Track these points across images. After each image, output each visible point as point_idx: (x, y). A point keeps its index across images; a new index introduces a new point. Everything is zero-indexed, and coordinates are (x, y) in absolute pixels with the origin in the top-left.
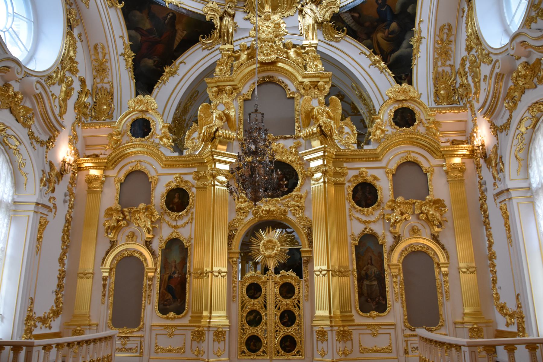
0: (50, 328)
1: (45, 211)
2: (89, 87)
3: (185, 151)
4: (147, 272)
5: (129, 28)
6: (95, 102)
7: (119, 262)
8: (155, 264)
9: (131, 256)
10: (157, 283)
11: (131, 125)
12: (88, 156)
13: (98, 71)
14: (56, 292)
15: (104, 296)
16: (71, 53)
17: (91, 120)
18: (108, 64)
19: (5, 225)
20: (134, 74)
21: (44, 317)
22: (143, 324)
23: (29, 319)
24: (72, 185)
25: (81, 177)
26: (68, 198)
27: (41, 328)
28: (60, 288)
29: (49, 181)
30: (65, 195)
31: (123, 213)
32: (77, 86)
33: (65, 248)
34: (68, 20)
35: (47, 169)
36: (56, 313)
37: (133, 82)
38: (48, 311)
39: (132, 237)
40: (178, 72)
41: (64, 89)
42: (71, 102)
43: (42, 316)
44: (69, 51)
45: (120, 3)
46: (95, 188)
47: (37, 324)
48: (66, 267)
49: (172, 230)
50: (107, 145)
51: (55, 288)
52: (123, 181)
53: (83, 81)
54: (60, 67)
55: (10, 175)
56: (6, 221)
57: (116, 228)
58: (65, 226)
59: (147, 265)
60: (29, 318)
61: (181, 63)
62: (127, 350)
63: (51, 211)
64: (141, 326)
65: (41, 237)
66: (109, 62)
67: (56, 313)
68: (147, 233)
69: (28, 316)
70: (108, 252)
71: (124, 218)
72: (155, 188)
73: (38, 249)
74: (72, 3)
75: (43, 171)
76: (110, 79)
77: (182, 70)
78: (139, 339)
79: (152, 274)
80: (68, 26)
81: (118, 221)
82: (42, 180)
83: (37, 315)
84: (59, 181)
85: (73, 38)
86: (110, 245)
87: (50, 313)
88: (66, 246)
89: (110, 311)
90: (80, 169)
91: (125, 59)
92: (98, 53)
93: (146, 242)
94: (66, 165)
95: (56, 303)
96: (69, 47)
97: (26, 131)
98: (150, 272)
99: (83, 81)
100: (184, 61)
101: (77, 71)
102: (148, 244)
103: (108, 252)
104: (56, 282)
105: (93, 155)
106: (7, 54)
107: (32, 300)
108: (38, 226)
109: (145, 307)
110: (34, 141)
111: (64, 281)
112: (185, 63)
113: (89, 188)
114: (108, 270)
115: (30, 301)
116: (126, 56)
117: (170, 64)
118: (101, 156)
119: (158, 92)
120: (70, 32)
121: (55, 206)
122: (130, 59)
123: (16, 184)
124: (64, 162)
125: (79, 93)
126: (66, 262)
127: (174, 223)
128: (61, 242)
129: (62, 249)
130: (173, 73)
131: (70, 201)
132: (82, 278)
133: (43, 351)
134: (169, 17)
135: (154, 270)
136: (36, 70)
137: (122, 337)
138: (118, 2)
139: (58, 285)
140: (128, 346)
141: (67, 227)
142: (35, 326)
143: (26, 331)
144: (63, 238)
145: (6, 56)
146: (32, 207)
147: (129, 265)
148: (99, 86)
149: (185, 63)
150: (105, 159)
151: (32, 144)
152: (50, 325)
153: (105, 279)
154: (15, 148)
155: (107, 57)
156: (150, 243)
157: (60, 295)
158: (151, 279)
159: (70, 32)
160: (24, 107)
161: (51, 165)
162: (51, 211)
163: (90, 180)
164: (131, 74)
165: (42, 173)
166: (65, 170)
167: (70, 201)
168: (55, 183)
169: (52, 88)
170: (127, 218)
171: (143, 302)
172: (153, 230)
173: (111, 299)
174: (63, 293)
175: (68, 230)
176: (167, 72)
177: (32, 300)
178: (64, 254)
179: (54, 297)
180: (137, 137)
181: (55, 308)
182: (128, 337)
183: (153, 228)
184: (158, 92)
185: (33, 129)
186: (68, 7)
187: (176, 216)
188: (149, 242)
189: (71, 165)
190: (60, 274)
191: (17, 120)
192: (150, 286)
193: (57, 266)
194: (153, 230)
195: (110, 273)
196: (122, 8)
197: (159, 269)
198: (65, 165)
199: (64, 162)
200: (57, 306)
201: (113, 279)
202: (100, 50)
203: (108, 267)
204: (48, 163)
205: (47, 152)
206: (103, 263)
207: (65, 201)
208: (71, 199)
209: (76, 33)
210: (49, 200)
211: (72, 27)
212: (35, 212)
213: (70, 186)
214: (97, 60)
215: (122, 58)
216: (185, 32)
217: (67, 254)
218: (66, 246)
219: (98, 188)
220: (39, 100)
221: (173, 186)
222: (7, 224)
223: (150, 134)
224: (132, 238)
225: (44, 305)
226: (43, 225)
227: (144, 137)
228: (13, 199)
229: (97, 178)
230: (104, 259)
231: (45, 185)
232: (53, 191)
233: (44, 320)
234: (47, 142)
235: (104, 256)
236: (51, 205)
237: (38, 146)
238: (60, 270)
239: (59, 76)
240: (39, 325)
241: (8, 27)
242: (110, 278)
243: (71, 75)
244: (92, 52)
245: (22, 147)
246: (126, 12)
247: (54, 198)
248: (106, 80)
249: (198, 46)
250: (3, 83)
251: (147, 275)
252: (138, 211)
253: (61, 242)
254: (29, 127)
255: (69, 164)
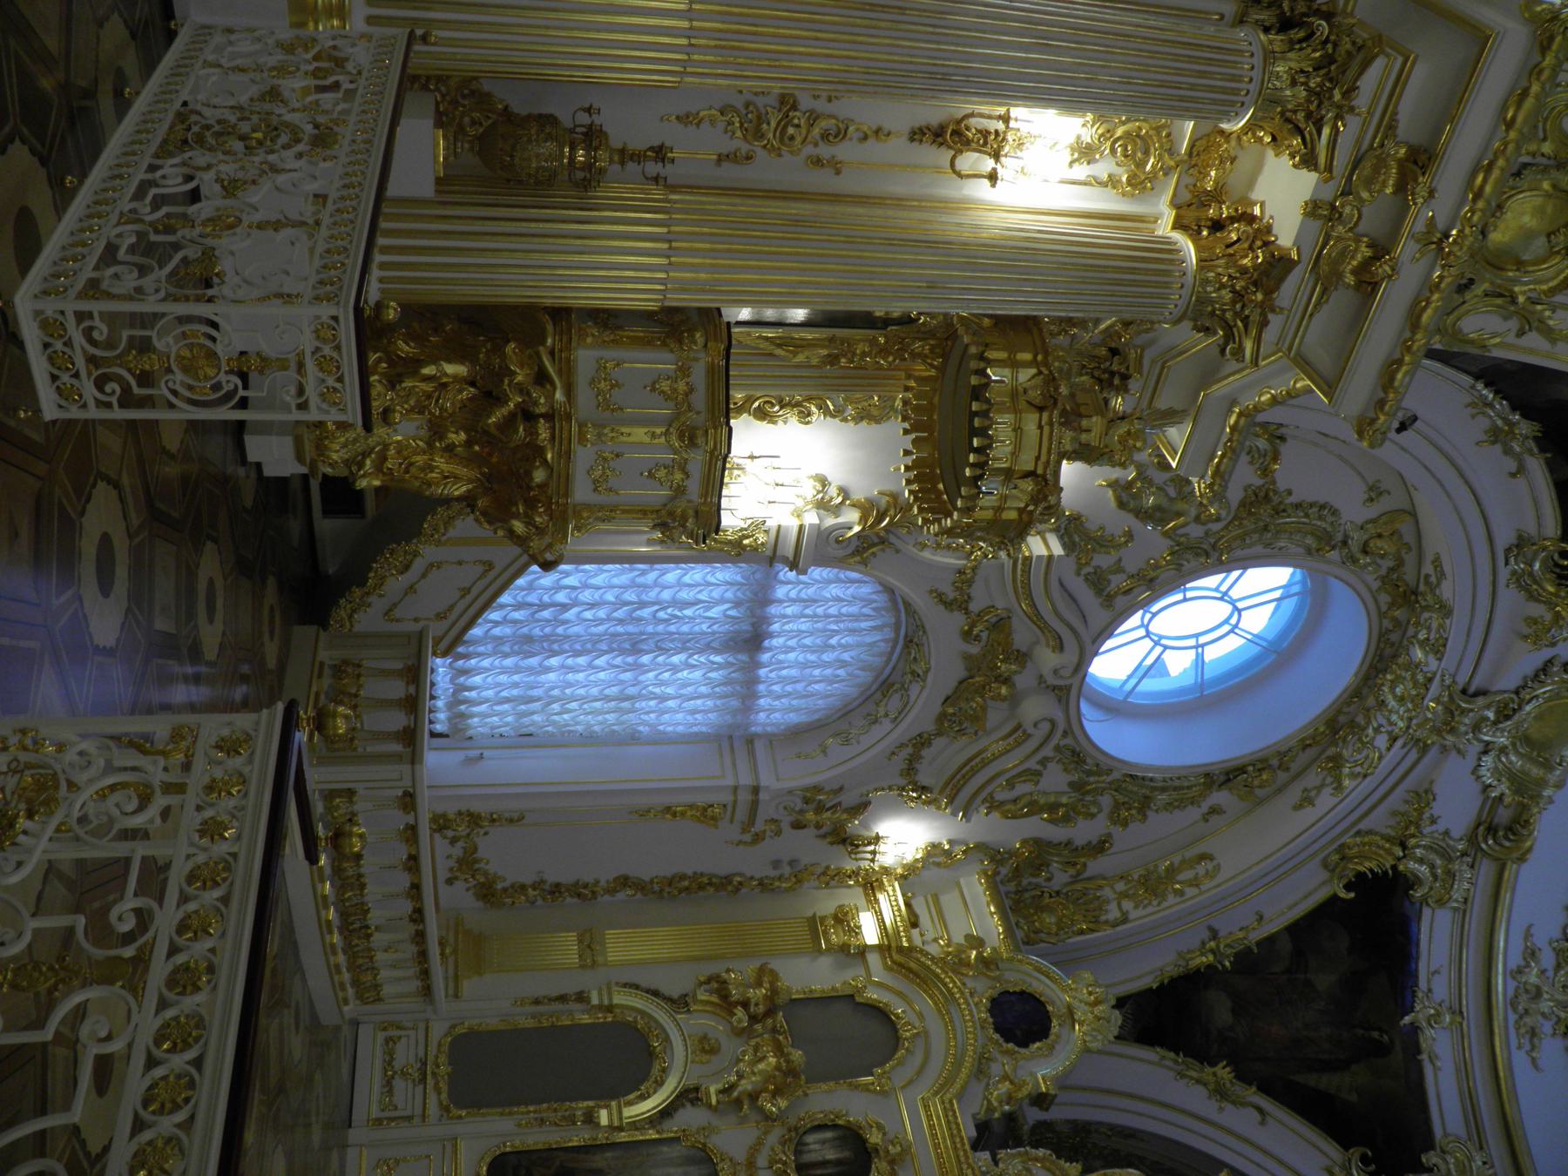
0: (450, 882)
1: (742, 813)
2: (1095, 866)
3: (986, 1155)
4: (607, 1107)
5: (1294, 929)
6: (1058, 893)
7: (632, 1027)
8: (635, 1126)
9: (651, 1055)
10: (578, 1137)
11: (1023, 993)
12: (908, 905)
13: (1145, 881)
14: (543, 881)
15: (537, 1002)
16: (1162, 798)
17: (1007, 894)
18: (1171, 899)
19: (695, 729)
20: (1173, 981)
21: (477, 861)
22: (460, 1117)
23: (469, 823)
24: (824, 873)
25: (852, 896)
26: (787, 870)
27: (449, 857)
28: (552, 893)
29: (820, 808)
30: (792, 863)
31: (770, 1012)
32: (1083, 831)
33: (656, 888)
34: (1242, 770)
35: (848, 799)
36: (488, 893)
37: (1149, 982)
38: (492, 868)
39: (706, 1047)
40: (1228, 1106)
41: (1064, 800)
42: (1037, 826)
43: (478, 855)
44: (1163, 790)
45: (1348, 887)
46: (825, 933)
47: (460, 844)
48: (607, 897)
49: (740, 1155)
50: (949, 940)
51: (552, 878)
52: (858, 999)
53: (1100, 847)
54: (1116, 775)
55: (816, 717)
56: (704, 729)
57: (726, 1002)
58: (711, 876)
59: (630, 1104)
60: (474, 819)
61: (1260, 1110)
62: (389, 1083)
63: (744, 831)
64: (455, 1112)
65: (674, 815)
66: (1178, 899)
67: (488, 893)
68: (720, 1086)
69: (479, 816)
70: (656, 993)
71: (754, 1019)
72: (857, 1087)
73: (644, 813)
74: (1288, 769)
75: (841, 789)
76: (1133, 915)
77: (1241, 1119)
78: (418, 1111)
79: (604, 1121)
80: (1227, 774)
81: (745, 1004)
82: (817, 789)
83: (482, 842)
84: (824, 836)
85: (1203, 796)
86: (675, 996)
87: (486, 874)
88: (661, 891)
89: (493, 1023)
90: (871, 885)
91: (1203, 944)
92: (1192, 868)
93: (697, 1089)
94: (871, 848)
95: (512, 886)
96: (1175, 789)
97: (930, 727)
98: (610, 1115)
99: (1100, 847)
100: (1268, 1118)
101: (1125, 824)
102: (689, 1096)
103: (656, 993)
104: (566, 878)
105: (916, 916)
106: (1094, 642)
107: (519, 820)
108: (701, 800)
109: (510, 1114)
110: (910, 750)
111: (569, 900)
112: (1263, 1123)
113: (823, 919)
114: (606, 1002)
115: (515, 816)
116: (1213, 944)
117: (1242, 1076)
118: (915, 932)
119: (1150, 1062)
120: (1213, 782)
121: (758, 838)
122: (1211, 958)
123: (795, 735)
124: (877, 839)
125: (1068, 843)
126: (620, 896)
127: (762, 1161)
128: (669, 875)
129: (652, 881)
130: (1220, 1093)
131: (780, 878)
132: (580, 942)
133: (400, 793)
134: (1376, 1034)
135: (616, 1124)
136: (1085, 723)
137: (425, 1064)
138: (1345, 881)
139: (558, 885)
140: (398, 1083)
141: (710, 884)
142: (453, 841)
143: (444, 816)
144: (683, 877)
145: (1087, 640)
146: (746, 780)
147: (625, 1056)
148: (1107, 892)
149: (1263, 1123)
150: (909, 940)
151: (902, 745)
152: (456, 878)
153: (581, 997)
154: (882, 713)
155: (1191, 891)
156: (695, 1101)
157: (531, 892)
158: (590, 1119)
159: (1213, 782)
160: (984, 709)
161: (860, 808)
162: (744, 831)
163: (843, 919)
164: (1173, 971)
165: (836, 787)
166: (857, 846)
167: (780, 878)
168: (818, 826)
169: (1053, 767)
170: (758, 1027)
171: (523, 1109)
172: (735, 1103)
173: (530, 1023)
174: (540, 902)
175: (701, 887)
176: (1215, 1074)
177: (519, 820)
178: (641, 886)
179: (527, 879)
180: (991, 1011)
181: (499, 886)
182: (423, 1080)
183: (738, 1103)
184: (1150, 1062)
185: (939, 743)
186: (1275, 762)
187: (785, 1163)
188: (698, 1099)
189: (873, 861)
190: (586, 886)
191: (948, 698)
192: (572, 1120)
193: (606, 875)
194: (735, 1103)
195: (600, 1007)
196: (1335, 897)
197: (623, 1137)
198: (869, 844)
199: (877, 839)
200: (505, 890)
201: (586, 1019)
202: (1202, 868)
203: (615, 1001)
204: (864, 799)
205: (890, 788)
206: (625, 985)
207: (776, 864)
208: (788, 879)
209: (1220, 797)
210: (773, 821)
211: (1230, 785)
212: (735, 789)
213: (819, 870)
214: (1172, 871)
215: (1206, 934)
216: (1354, 1098)
217: (639, 895)
218: (661, 891)
219: (827, 941)
220: (1011, 740)
221: (874, 1138)
222: (696, 734)
223: (1010, 1045)
224: (703, 1051)
225: (504, 857)
226: (706, 815)
227: (997, 1030)
228: (758, 736)
229: (856, 931)
230: (637, 987)
231: (807, 801)
232: (798, 826)
233: (468, 863)
234: (915, 783)
235: (644, 985)
236: (759, 826)
237: (900, 761)
238: (597, 882)
239: (1092, 779)
240: (457, 851)
241: (1164, 642)
242: (588, 1012)
243: (1106, 810)
244: (1190, 853)
245: (887, 725)
246: (1328, 910)
247: (778, 833)
248: (1127, 905)
249: (1333, 1150)
250: (1024, 649)
251: (600, 1107)
252: (779, 1050)
253: (668, 871)
254: (939, 734)
255: (874, 853)
